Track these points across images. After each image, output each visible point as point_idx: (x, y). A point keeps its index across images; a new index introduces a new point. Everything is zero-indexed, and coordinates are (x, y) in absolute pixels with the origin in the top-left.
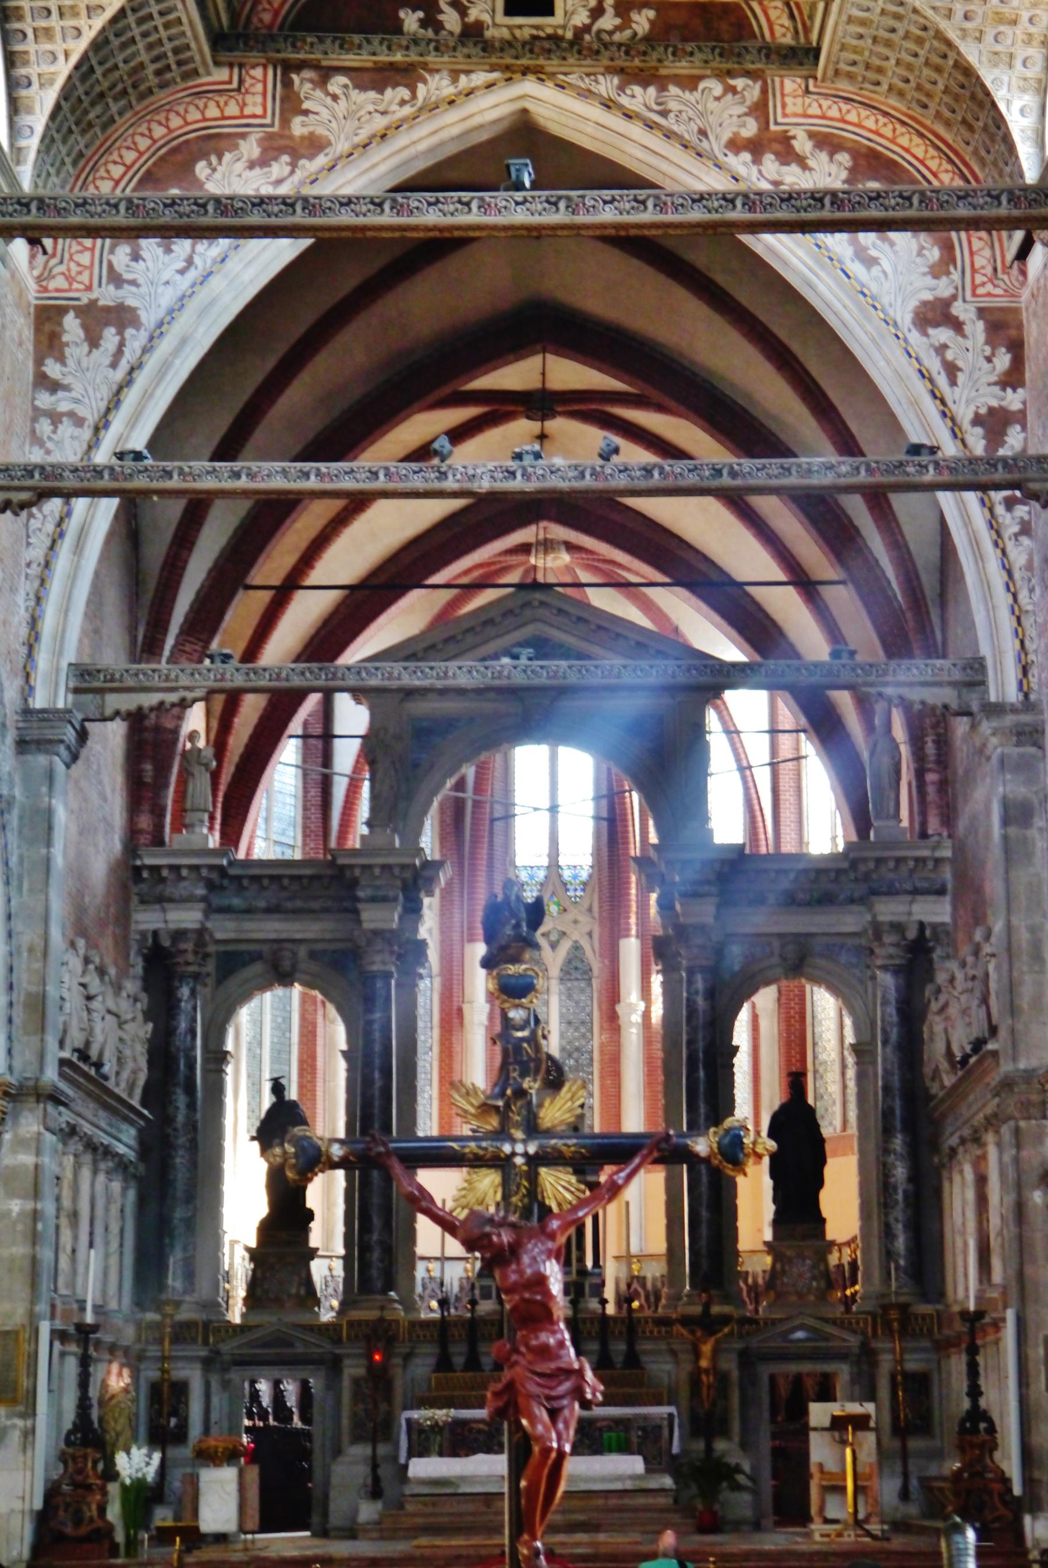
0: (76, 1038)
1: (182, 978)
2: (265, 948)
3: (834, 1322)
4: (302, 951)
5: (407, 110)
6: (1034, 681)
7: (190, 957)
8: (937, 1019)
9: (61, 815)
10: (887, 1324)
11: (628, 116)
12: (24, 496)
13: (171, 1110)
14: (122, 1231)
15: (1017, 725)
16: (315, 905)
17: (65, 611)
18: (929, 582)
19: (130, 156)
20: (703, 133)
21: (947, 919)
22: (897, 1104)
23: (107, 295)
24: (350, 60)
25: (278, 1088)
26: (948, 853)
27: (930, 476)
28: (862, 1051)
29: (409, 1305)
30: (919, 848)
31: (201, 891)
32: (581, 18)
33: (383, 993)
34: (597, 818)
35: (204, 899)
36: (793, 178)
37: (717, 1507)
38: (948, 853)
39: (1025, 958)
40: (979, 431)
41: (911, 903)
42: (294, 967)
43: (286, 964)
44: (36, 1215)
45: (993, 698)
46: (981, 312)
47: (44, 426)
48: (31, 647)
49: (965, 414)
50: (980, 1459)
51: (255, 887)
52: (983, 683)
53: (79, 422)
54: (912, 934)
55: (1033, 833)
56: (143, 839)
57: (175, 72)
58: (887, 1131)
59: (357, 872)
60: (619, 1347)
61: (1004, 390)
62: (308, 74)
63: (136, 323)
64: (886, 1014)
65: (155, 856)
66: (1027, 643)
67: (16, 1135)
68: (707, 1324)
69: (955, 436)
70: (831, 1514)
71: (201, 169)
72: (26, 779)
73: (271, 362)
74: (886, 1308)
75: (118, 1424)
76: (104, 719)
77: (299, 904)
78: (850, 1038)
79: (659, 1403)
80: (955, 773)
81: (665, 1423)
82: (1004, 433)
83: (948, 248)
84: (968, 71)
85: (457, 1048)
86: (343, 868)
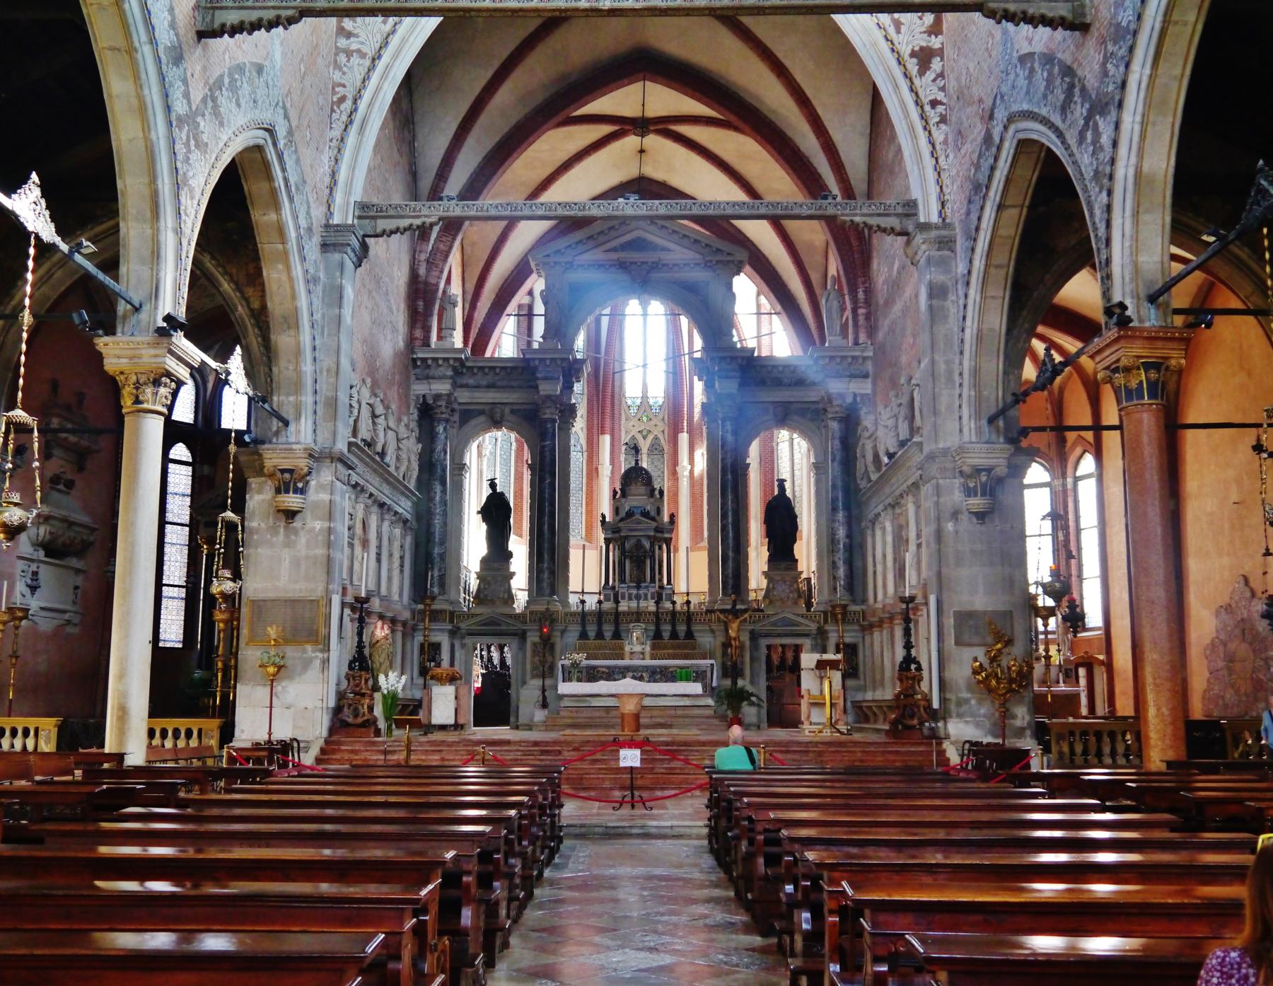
1: (439, 420)
2: (487, 408)
4: (507, 410)
6: (948, 211)
7: (444, 409)
8: (868, 442)
9: (349, 292)
10: (834, 615)
12: (290, 13)
13: (432, 494)
14: (402, 558)
15: (939, 237)
16: (515, 384)
17: (353, 168)
21: (869, 391)
25: (493, 485)
26: (871, 354)
28: (818, 468)
29: (565, 603)
30: (854, 350)
31: (450, 373)
33: (551, 430)
34: (667, 372)
35: (451, 377)
37: (740, 716)
38: (871, 354)
39: (943, 380)
40: (915, 60)
41: (850, 382)
42: (502, 416)
43: (498, 416)
44: (330, 531)
45: (922, 220)
47: (342, 58)
48: (331, 190)
49: (906, 51)
50: (913, 687)
51: (480, 373)
52: (915, 215)
53: (363, 55)
55: (948, 304)
56: (418, 343)
59: (537, 363)
60: (682, 628)
61: (930, 36)
65: (424, 352)
66: (944, 188)
67: (318, 481)
68: (735, 613)
69: (900, 63)
70: (814, 719)
72: (327, 268)
73: (490, 74)
74: (834, 607)
75: (380, 658)
76: (377, 236)
77: (505, 383)
78: (813, 460)
79: (705, 658)
80: (877, 305)
81: (709, 669)
82: (929, 62)
85: (595, 488)
86: (528, 360)
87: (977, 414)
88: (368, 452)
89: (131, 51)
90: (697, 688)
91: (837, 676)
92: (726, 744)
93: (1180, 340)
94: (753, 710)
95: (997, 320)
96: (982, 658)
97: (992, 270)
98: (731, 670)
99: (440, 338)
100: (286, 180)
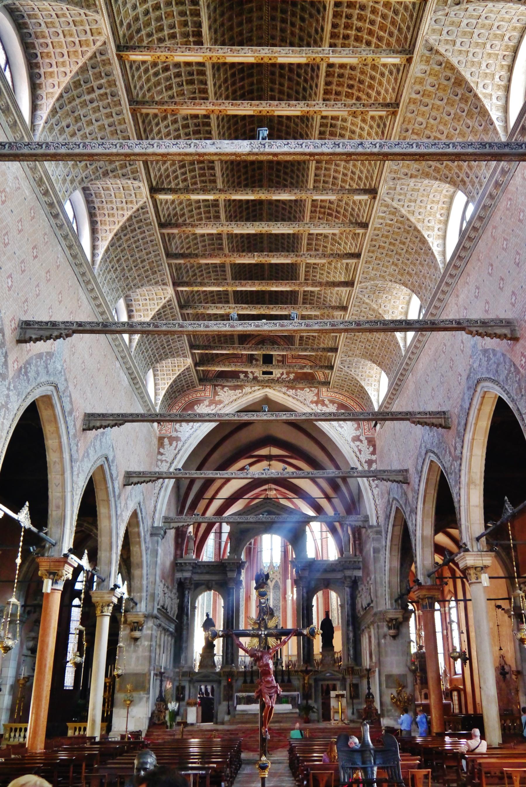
0: (161, 603)
3: (336, 671)
4: (214, 583)
5: (241, 395)
9: (160, 551)
11: (289, 396)
12: (154, 479)
17: (162, 504)
18: (356, 498)
19: (180, 404)
20: (305, 399)
21: (361, 575)
22: (350, 619)
23: (174, 434)
24: (229, 384)
25: (207, 615)
26: (361, 560)
27: (356, 474)
28: (342, 606)
29: (237, 667)
31: (191, 568)
32: (279, 375)
35: (192, 570)
36: (325, 410)
43: (210, 586)
46: (366, 438)
47: (159, 463)
49: (363, 461)
53: (167, 462)
54: (353, 579)
55: (380, 555)
56: (178, 556)
57: (191, 387)
58: (348, 625)
60: (286, 678)
62: (219, 387)
63: (180, 440)
64: (347, 597)
68: (307, 672)
70: (336, 719)
71: (196, 407)
72: (152, 542)
74: (348, 668)
78: (339, 603)
79: (295, 691)
83: (359, 424)
84: (362, 387)
86: (223, 563)
87: (391, 598)
88: (163, 610)
89: (108, 501)
90: (289, 706)
91: (344, 700)
92: (293, 729)
93: (439, 589)
94: (316, 714)
95: (396, 564)
96: (395, 694)
97: (394, 547)
98: (306, 696)
99: (186, 553)
100: (142, 517)
